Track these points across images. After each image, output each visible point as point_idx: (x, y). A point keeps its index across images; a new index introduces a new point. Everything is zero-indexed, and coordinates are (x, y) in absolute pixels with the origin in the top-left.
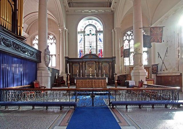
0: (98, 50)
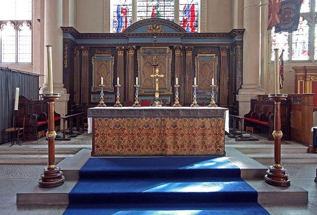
0: (181, 8)
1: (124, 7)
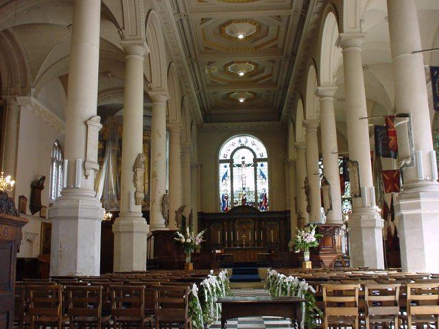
0: (259, 196)
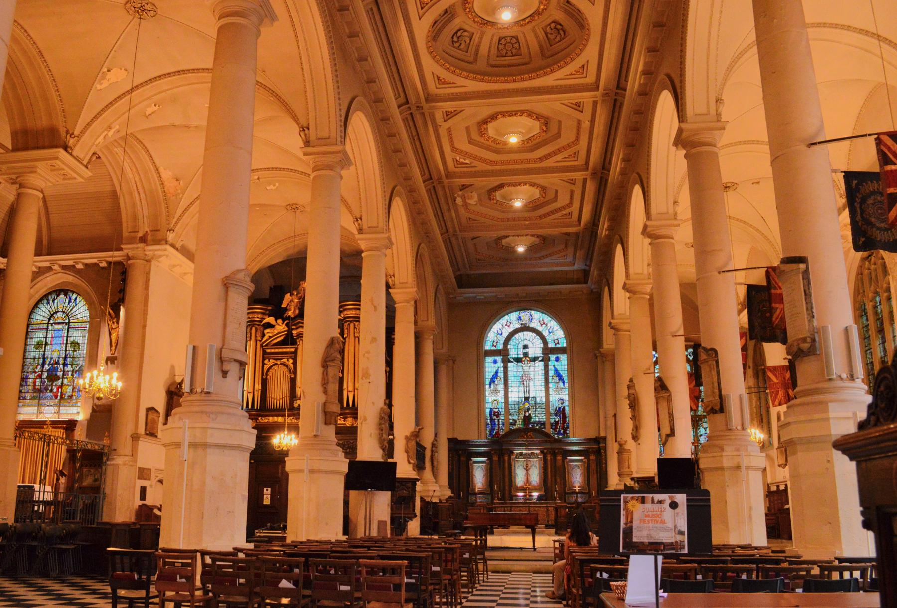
1: (496, 410)
